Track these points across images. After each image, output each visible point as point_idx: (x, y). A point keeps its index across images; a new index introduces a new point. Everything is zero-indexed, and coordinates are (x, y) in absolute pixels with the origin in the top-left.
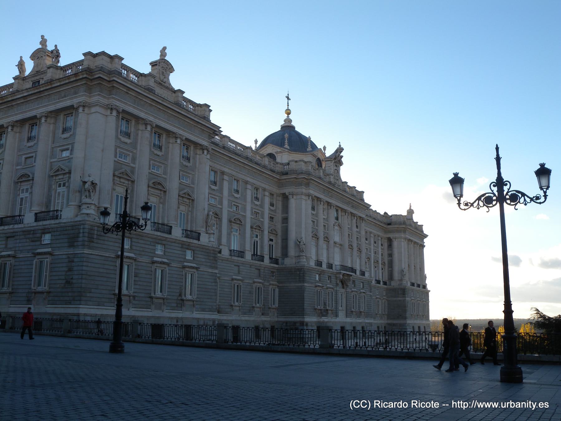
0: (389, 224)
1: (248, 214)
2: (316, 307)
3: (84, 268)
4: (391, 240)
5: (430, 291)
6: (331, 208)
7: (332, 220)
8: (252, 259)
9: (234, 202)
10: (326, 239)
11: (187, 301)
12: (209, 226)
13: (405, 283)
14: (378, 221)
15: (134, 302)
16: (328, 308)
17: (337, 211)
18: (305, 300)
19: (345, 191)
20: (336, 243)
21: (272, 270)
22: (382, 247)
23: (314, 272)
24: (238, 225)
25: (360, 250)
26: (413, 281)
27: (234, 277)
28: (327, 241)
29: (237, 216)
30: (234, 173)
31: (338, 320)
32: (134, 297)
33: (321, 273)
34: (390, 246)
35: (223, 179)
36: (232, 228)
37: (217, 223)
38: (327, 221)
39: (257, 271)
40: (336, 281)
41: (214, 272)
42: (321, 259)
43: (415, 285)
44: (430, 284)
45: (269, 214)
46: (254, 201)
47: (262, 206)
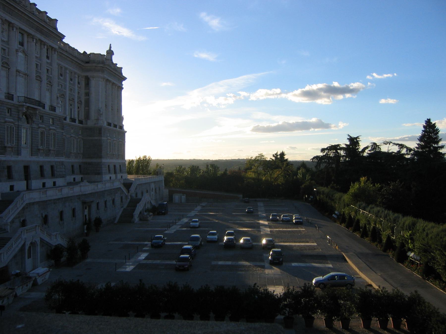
0: (87, 62)
4: (89, 78)
5: (126, 132)
6: (13, 30)
10: (6, 66)
13: (102, 122)
14: (75, 57)
16: (6, 145)
17: (22, 34)
19: (33, 14)
22: (79, 86)
25: (50, 83)
26: (110, 122)
31: (19, 158)
34: (88, 84)
38: (8, 45)
40: (18, 115)
43: (112, 125)
44: (127, 125)
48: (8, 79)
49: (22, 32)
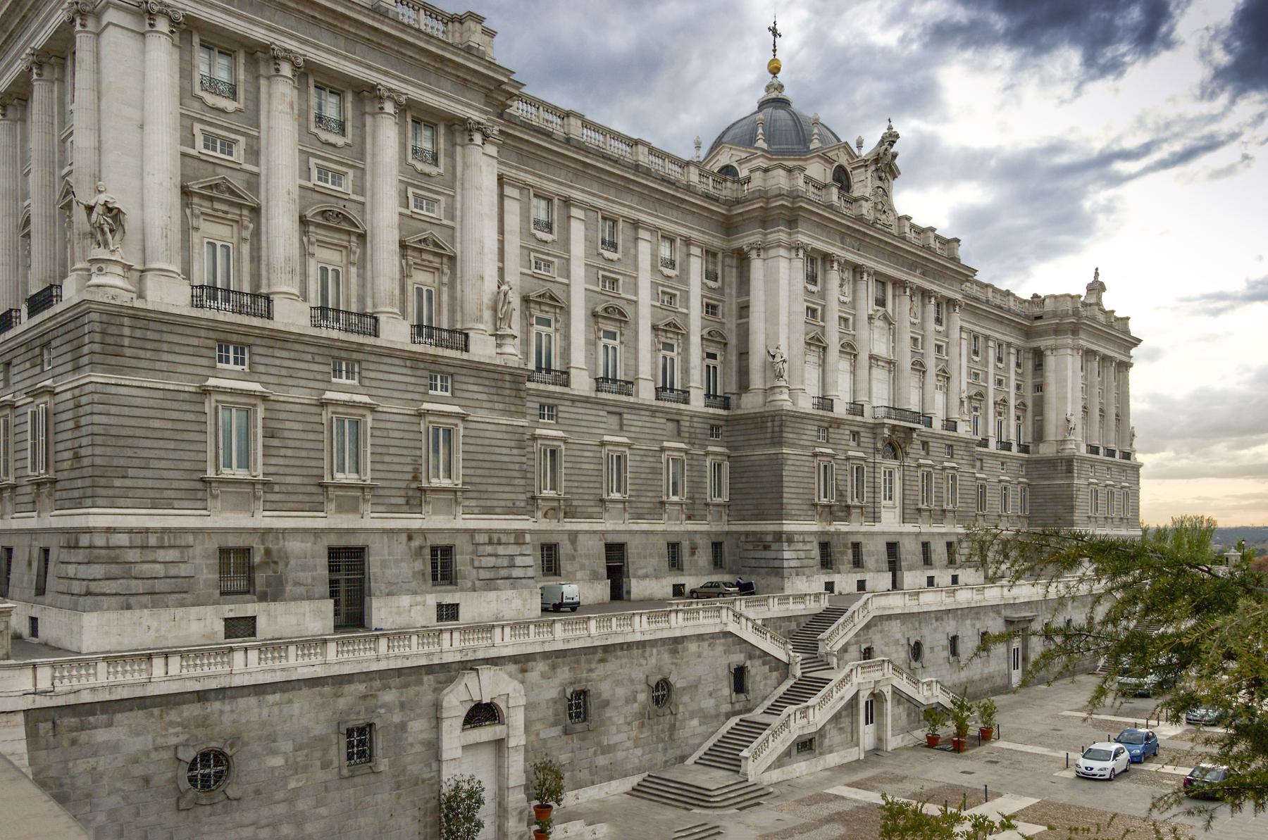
1: (645, 297)
2: (816, 500)
3: (96, 419)
7: (867, 306)
8: (657, 399)
9: (604, 270)
10: (848, 350)
11: (432, 491)
12: (501, 319)
15: (270, 497)
18: (785, 484)
19: (904, 238)
20: (877, 360)
21: (712, 422)
23: (811, 422)
24: (618, 324)
27: (606, 438)
28: (851, 354)
29: (613, 302)
30: (600, 203)
32: (265, 483)
33: (829, 426)
35: (569, 217)
36: (599, 330)
37: (556, 320)
39: (671, 425)
41: (515, 423)
42: (831, 393)
45: (703, 296)
46: (662, 269)
47: (684, 278)
48: (854, 375)
49: (882, 280)
